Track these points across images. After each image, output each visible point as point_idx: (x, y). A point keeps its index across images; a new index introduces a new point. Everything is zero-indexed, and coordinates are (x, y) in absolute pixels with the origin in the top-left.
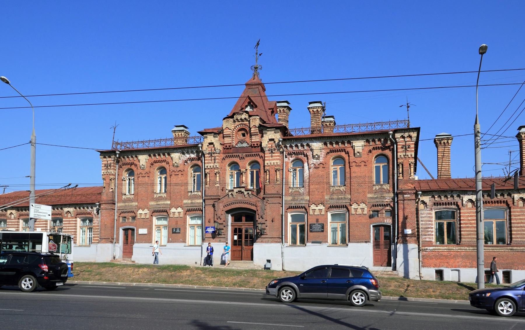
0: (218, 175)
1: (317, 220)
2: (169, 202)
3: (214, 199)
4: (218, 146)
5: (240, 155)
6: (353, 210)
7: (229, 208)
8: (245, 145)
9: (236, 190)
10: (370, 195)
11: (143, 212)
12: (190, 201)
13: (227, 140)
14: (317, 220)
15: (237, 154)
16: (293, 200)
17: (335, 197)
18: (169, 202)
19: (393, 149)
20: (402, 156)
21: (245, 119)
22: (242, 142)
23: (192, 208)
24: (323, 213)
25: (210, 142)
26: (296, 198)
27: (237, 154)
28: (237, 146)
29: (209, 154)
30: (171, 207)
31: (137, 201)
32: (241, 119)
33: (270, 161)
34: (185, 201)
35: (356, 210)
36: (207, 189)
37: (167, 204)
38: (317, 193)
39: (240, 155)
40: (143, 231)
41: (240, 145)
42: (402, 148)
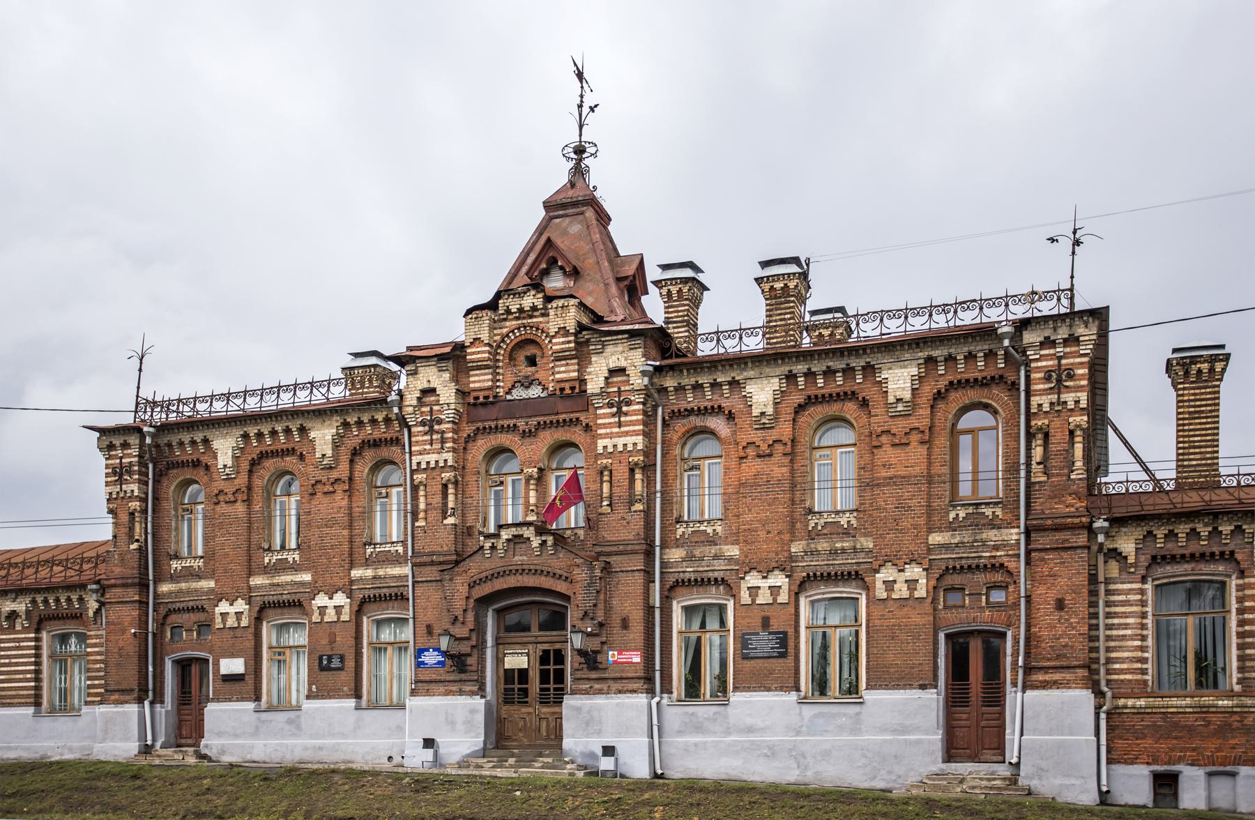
0: (451, 490)
1: (766, 623)
2: (307, 577)
3: (441, 563)
5: (521, 424)
6: (879, 585)
7: (487, 589)
8: (535, 392)
9: (505, 535)
11: (232, 610)
12: (369, 573)
13: (479, 381)
14: (766, 623)
15: (512, 422)
16: (690, 558)
17: (823, 545)
18: (307, 577)
19: (1014, 386)
20: (1046, 408)
21: (534, 308)
22: (528, 383)
23: (377, 592)
24: (783, 597)
25: (426, 385)
26: (697, 553)
27: (512, 422)
28: (509, 397)
29: (423, 423)
31: (211, 575)
32: (521, 310)
33: (615, 440)
36: (419, 533)
37: (302, 584)
38: (762, 534)
39: (521, 424)
40: (233, 666)
41: (519, 393)
42: (1048, 379)
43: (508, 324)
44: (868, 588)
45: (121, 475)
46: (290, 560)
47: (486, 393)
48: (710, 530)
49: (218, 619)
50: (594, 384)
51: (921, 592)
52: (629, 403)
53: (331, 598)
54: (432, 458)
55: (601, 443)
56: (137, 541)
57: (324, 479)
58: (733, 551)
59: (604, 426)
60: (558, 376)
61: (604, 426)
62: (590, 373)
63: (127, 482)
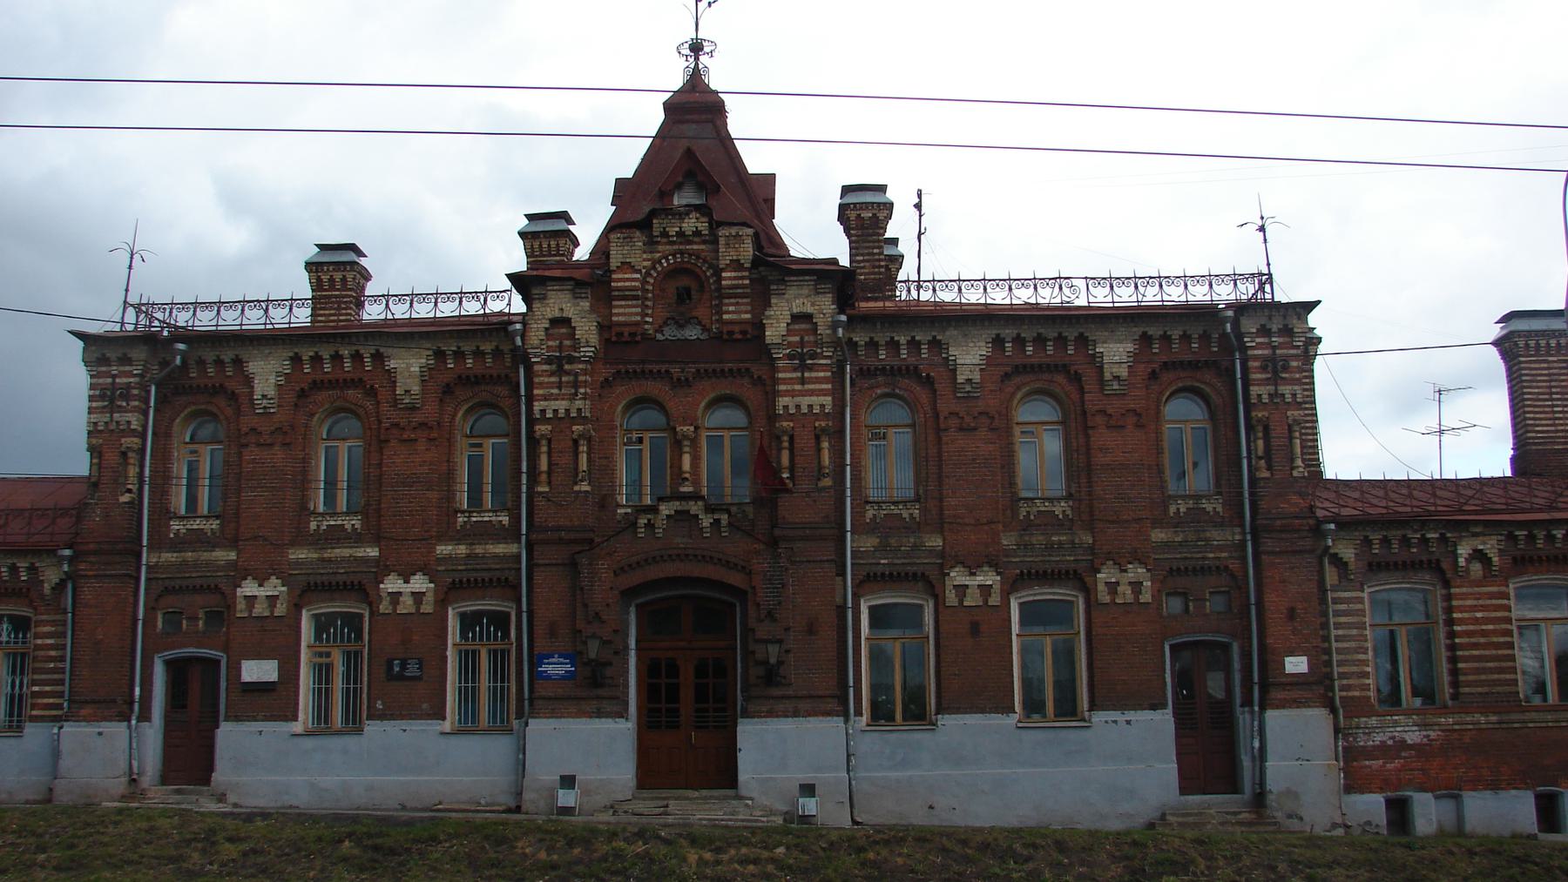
0: (583, 448)
2: (373, 552)
3: (574, 541)
4: (587, 331)
5: (675, 370)
6: (1101, 587)
7: (634, 578)
8: (692, 333)
9: (666, 509)
10: (1158, 535)
11: (262, 592)
12: (462, 550)
13: (624, 313)
15: (663, 368)
16: (883, 548)
17: (1038, 539)
18: (373, 552)
20: (1265, 399)
21: (697, 233)
23: (472, 575)
24: (995, 600)
25: (557, 314)
26: (893, 541)
27: (663, 368)
28: (659, 337)
29: (549, 361)
30: (381, 569)
31: (234, 543)
32: (681, 234)
33: (798, 399)
34: (443, 549)
35: (1113, 587)
36: (540, 502)
37: (365, 560)
39: (675, 370)
43: (660, 248)
44: (1088, 591)
45: (112, 401)
46: (348, 527)
47: (633, 329)
48: (905, 514)
49: (241, 605)
50: (775, 330)
51: (1146, 597)
52: (814, 356)
53: (407, 582)
54: (561, 405)
55: (783, 401)
56: (129, 491)
57: (403, 422)
58: (935, 542)
59: (785, 381)
60: (725, 317)
61: (785, 381)
62: (769, 317)
63: (121, 409)
